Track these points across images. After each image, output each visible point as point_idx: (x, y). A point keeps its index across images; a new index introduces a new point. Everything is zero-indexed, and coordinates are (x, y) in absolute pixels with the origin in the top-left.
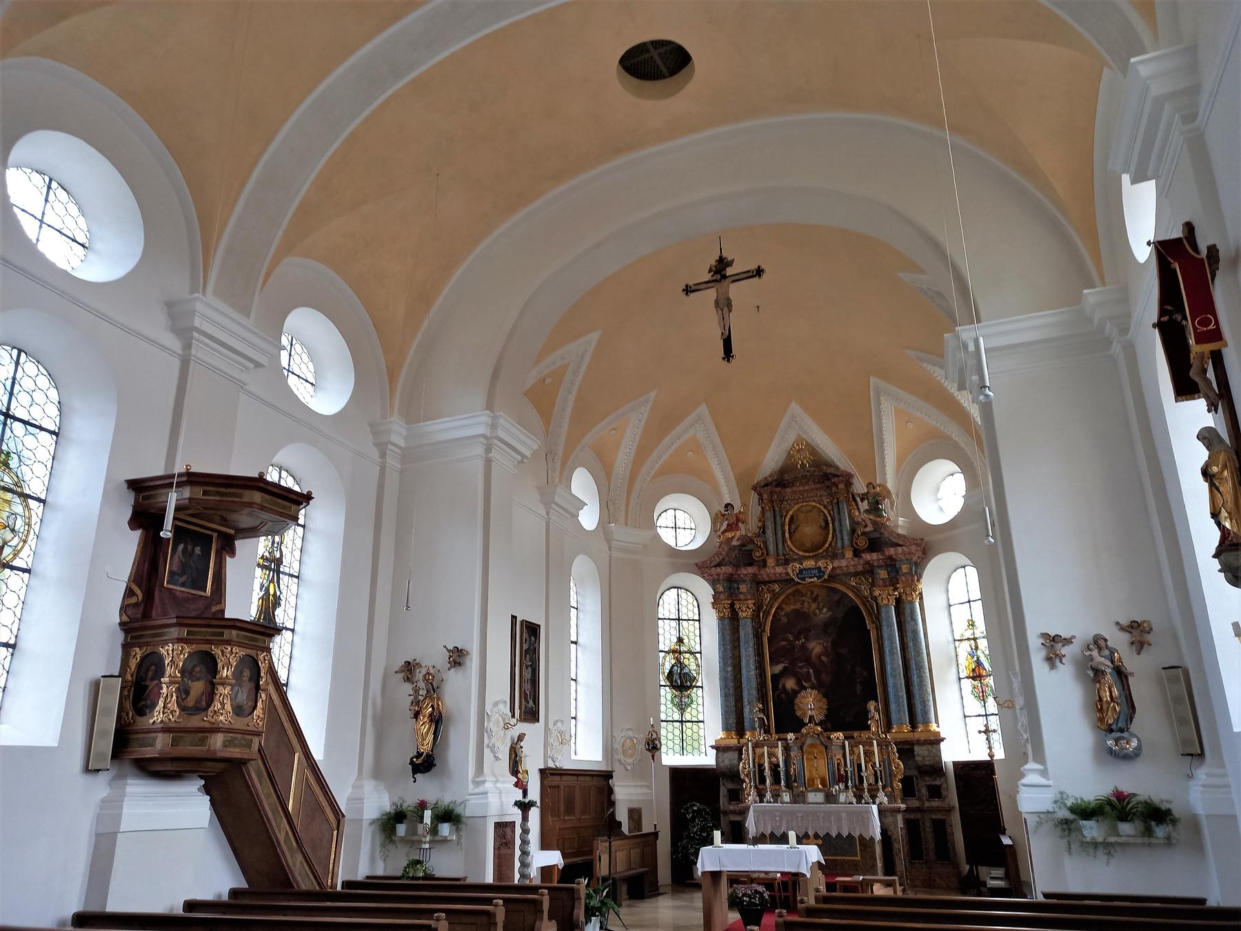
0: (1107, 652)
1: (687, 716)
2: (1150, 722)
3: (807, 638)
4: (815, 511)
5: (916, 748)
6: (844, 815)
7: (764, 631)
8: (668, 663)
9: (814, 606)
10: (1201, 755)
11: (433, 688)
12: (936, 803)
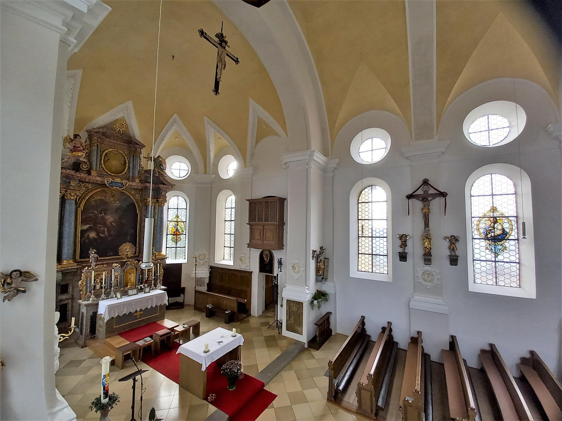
3: (105, 214)
9: (112, 199)
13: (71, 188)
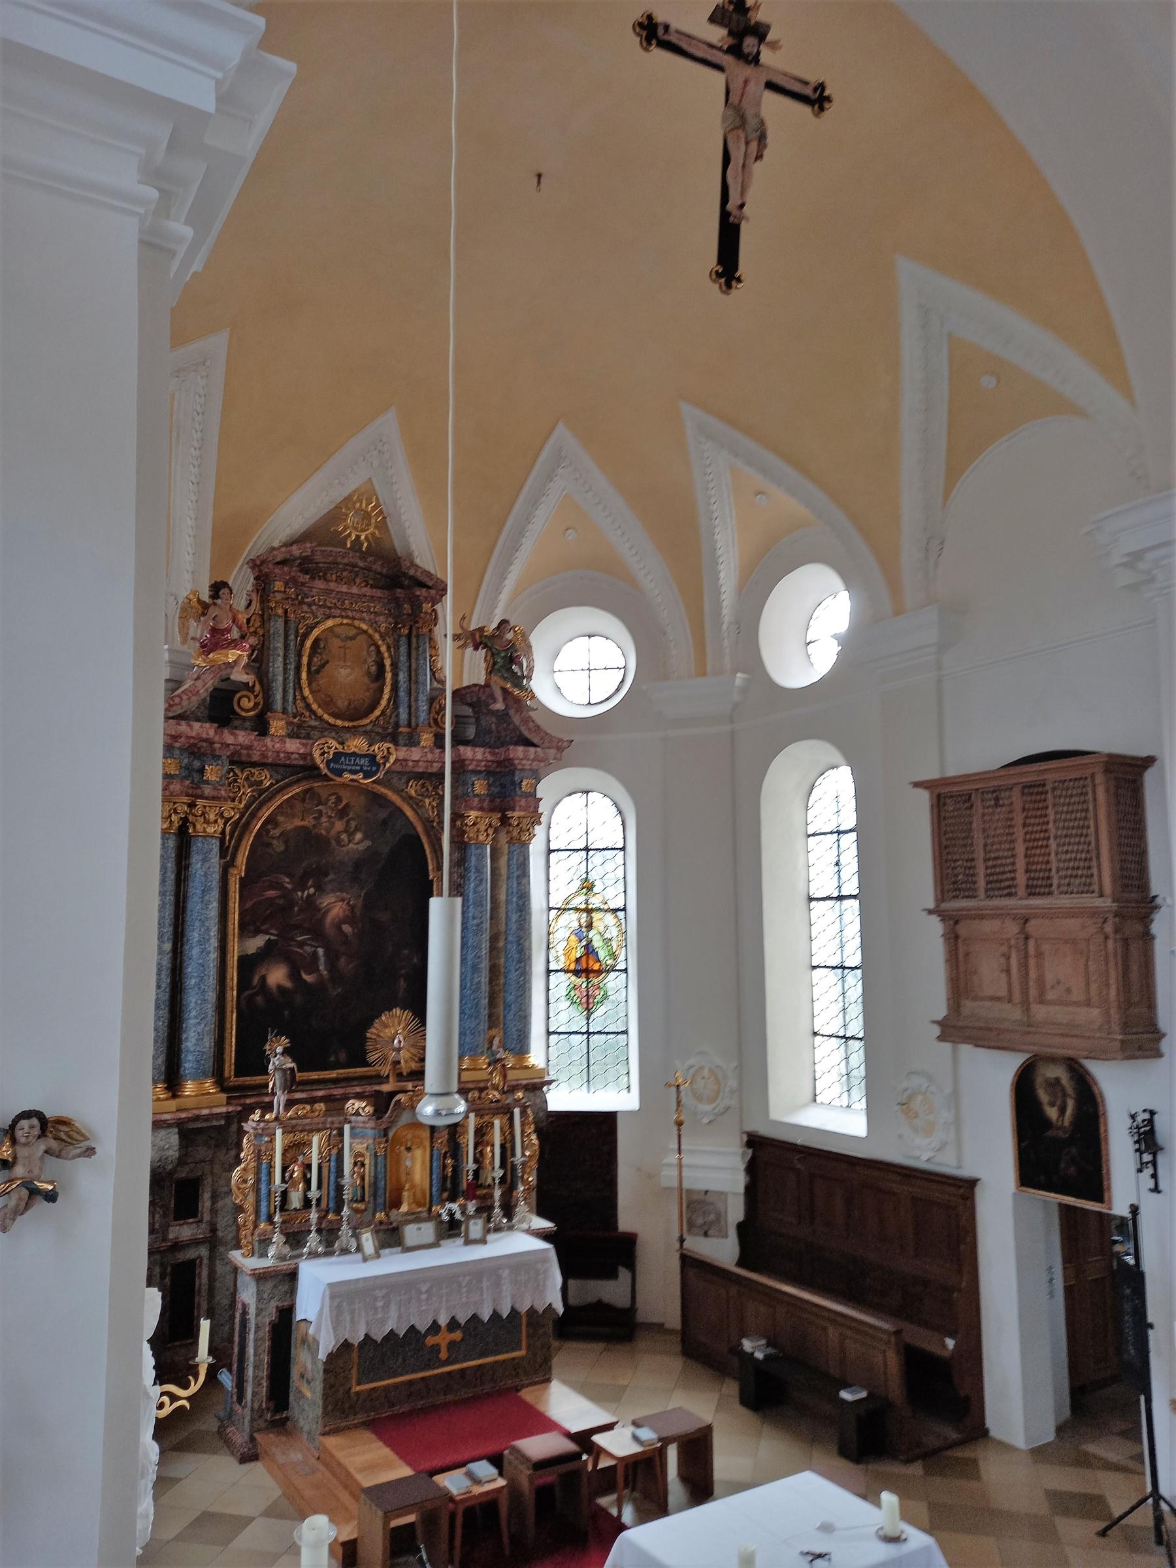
3: (319, 888)
4: (362, 638)
6: (505, 1273)
9: (339, 825)
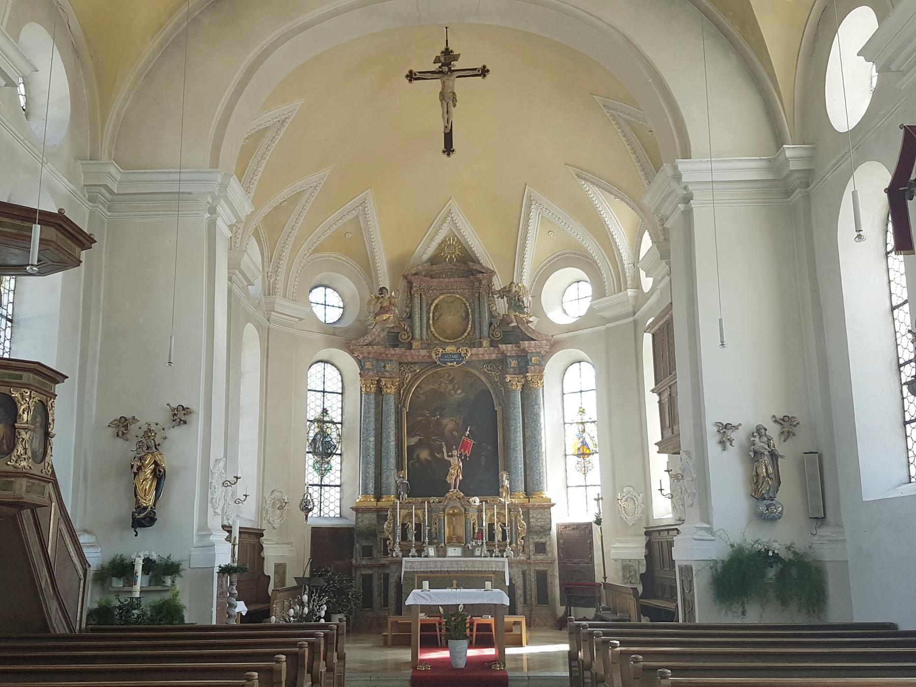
0: (765, 439)
1: (326, 481)
2: (788, 496)
5: (531, 512)
7: (404, 406)
8: (314, 430)
9: (450, 387)
10: (825, 517)
11: (149, 443)
12: (540, 557)
13: (387, 374)
